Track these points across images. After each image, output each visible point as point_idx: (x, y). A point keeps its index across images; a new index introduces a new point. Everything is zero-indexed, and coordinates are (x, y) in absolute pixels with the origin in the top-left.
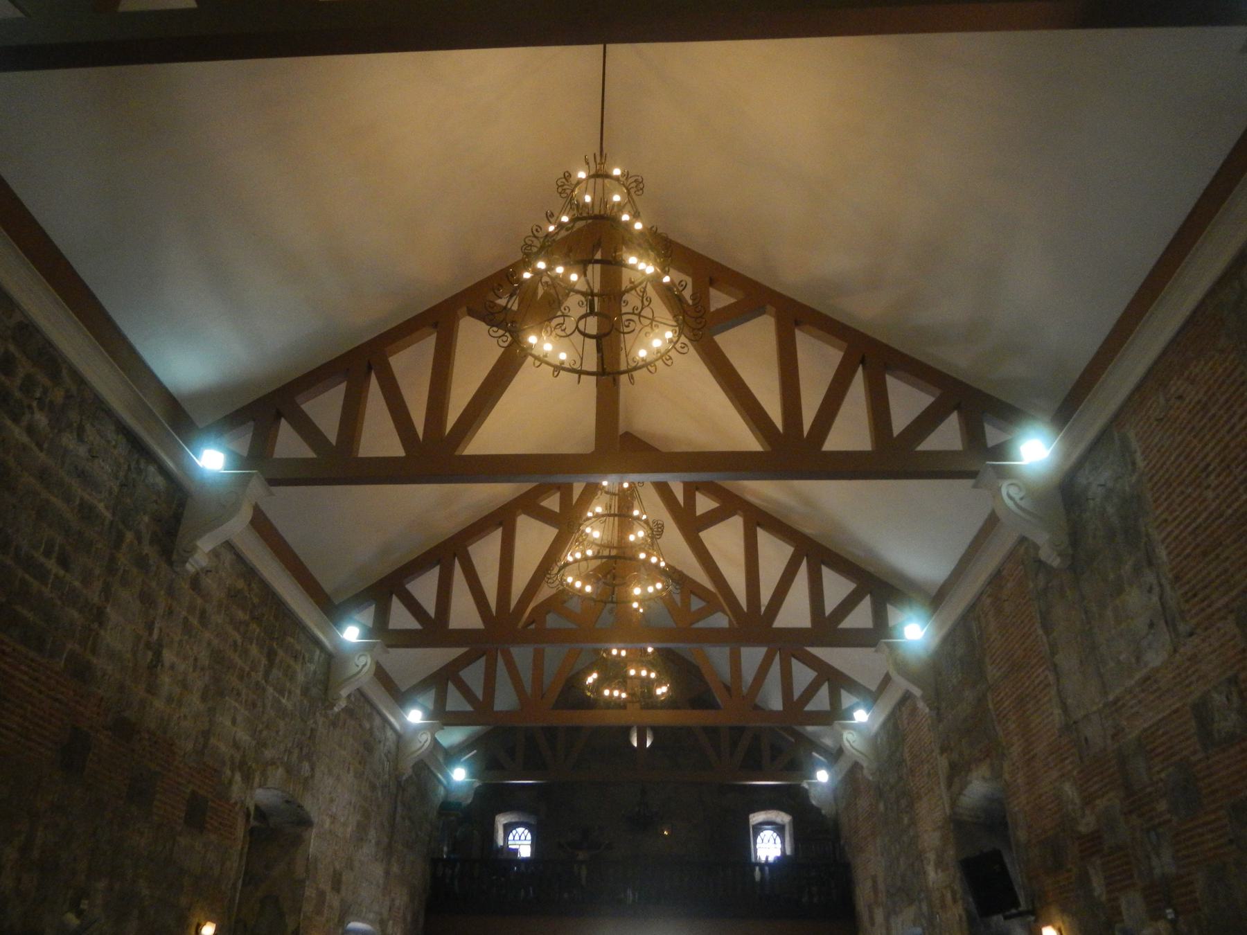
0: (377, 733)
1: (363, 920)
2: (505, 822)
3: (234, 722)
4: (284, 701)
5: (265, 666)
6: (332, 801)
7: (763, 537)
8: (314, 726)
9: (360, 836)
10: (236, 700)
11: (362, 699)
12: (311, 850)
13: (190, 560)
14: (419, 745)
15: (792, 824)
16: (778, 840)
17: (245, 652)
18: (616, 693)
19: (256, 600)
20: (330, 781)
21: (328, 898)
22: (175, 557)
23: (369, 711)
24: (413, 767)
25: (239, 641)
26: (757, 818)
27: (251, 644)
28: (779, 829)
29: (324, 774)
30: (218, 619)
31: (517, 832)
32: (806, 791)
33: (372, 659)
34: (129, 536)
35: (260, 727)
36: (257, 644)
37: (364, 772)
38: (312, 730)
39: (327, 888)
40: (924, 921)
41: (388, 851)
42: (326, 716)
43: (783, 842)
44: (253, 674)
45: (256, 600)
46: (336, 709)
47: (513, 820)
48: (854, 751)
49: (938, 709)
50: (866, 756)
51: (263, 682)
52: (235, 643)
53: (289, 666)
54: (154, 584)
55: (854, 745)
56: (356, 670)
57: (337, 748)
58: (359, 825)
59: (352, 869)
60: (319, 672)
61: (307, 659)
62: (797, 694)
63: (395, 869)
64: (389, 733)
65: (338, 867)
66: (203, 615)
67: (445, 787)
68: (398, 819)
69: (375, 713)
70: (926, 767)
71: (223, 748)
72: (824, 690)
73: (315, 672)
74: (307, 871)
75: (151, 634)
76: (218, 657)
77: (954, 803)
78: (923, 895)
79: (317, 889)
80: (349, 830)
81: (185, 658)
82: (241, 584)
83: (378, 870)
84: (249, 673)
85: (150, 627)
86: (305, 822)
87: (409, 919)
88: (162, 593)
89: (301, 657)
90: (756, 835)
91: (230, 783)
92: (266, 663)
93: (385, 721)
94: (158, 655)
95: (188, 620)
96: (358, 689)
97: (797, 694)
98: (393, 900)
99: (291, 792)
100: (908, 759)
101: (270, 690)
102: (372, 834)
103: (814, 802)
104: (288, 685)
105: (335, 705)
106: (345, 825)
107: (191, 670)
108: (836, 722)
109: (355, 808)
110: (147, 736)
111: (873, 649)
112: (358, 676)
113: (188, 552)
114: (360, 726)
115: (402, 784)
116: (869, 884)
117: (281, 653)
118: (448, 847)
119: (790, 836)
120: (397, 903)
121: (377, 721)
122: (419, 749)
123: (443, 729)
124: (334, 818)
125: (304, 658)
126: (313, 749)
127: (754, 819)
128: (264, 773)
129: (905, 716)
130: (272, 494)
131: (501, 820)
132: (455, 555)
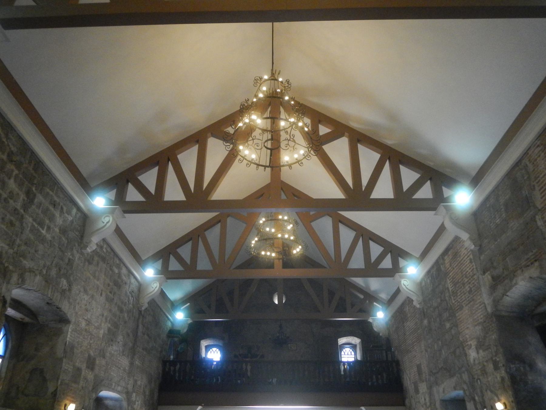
0: (124, 278)
1: (113, 390)
2: (206, 345)
4: (44, 232)
5: (24, 200)
6: (87, 310)
7: (362, 150)
8: (71, 257)
9: (111, 337)
11: (112, 253)
12: (68, 339)
15: (361, 343)
16: (353, 353)
18: (268, 254)
19: (14, 149)
20: (86, 297)
21: (83, 373)
23: (118, 262)
24: (148, 303)
26: (342, 341)
27: (9, 178)
28: (354, 347)
29: (80, 292)
31: (212, 350)
33: (114, 219)
35: (18, 241)
37: (113, 299)
38: (69, 260)
39: (84, 366)
40: (465, 387)
41: (132, 352)
42: (82, 254)
43: (355, 354)
44: (11, 201)
46: (89, 250)
47: (210, 344)
49: (480, 246)
50: (416, 294)
51: (22, 211)
53: (48, 209)
56: (102, 225)
57: (92, 277)
58: (109, 330)
59: (104, 357)
60: (75, 223)
61: (65, 211)
62: (373, 259)
63: (137, 363)
64: (133, 280)
67: (171, 322)
68: (140, 334)
69: (122, 265)
70: (467, 287)
72: (389, 257)
73: (72, 222)
74: (65, 352)
77: (496, 303)
78: (464, 369)
79: (74, 366)
80: (102, 332)
83: (125, 362)
86: (64, 320)
87: (147, 393)
89: (60, 207)
90: (341, 350)
93: (130, 273)
97: (373, 259)
98: (136, 381)
99: (49, 296)
100: (450, 287)
101: (29, 220)
102: (120, 338)
103: (375, 329)
104: (47, 222)
105: (87, 246)
106: (98, 328)
108: (397, 274)
109: (106, 319)
111: (434, 212)
112: (104, 229)
114: (111, 269)
115: (143, 313)
116: (415, 369)
117: (39, 198)
118: (173, 355)
119: (360, 350)
120: (139, 383)
121: (124, 271)
122: (152, 292)
123: (167, 282)
124: (89, 322)
125: (62, 208)
126: (70, 272)
127: (340, 341)
128: (22, 276)
129: (446, 262)
131: (204, 343)
132: (169, 160)
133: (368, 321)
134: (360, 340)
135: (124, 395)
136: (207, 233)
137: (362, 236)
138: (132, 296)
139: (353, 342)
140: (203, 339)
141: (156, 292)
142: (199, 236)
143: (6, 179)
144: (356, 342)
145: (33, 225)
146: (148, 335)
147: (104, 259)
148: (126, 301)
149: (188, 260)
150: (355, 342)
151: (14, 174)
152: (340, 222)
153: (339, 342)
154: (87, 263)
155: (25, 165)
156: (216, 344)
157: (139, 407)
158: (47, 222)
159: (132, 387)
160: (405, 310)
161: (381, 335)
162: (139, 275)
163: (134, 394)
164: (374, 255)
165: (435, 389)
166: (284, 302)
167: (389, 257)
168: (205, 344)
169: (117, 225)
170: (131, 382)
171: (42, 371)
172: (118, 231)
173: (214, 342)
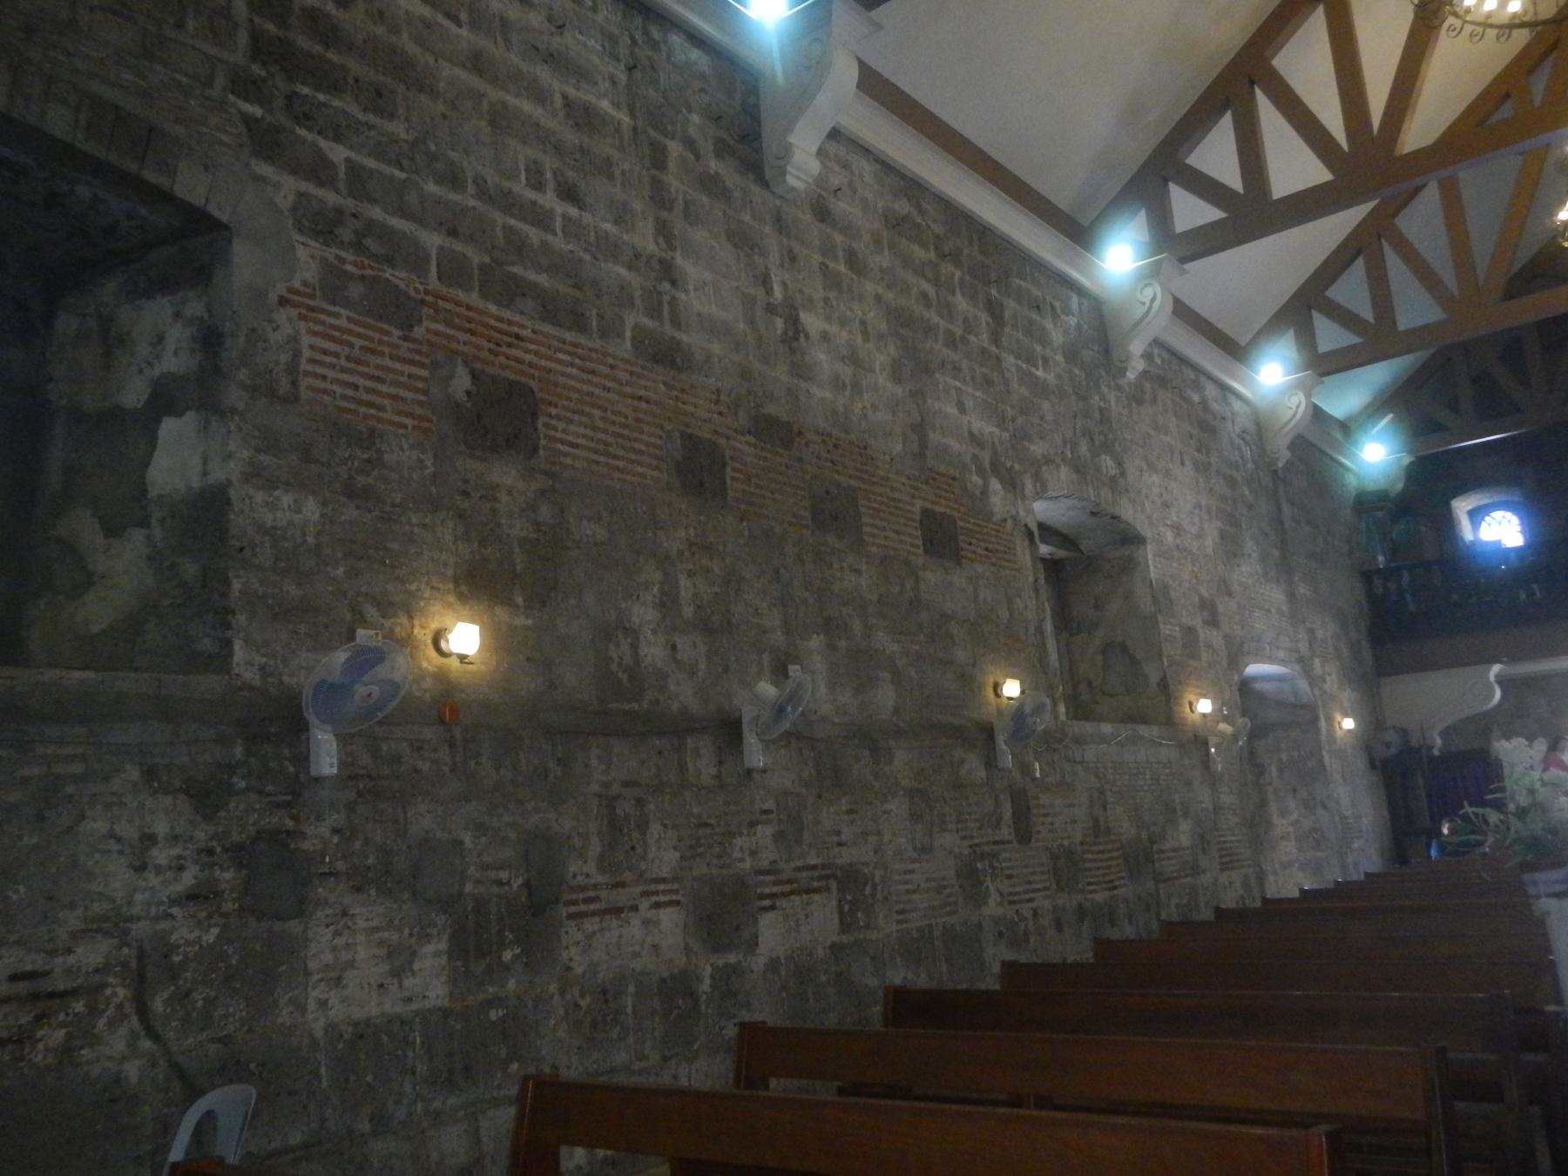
0: (1215, 407)
1: (1270, 660)
2: (1469, 508)
3: (962, 408)
4: (1040, 373)
5: (988, 324)
6: (1166, 505)
8: (1102, 404)
9: (1230, 546)
10: (955, 378)
11: (1175, 361)
12: (1152, 575)
13: (789, 168)
17: (947, 310)
20: (1155, 478)
22: (768, 174)
23: (1192, 376)
24: (1288, 448)
25: (931, 292)
27: (954, 294)
29: (1141, 471)
30: (884, 260)
33: (1164, 288)
34: (674, 148)
35: (1010, 412)
36: (963, 294)
38: (1101, 411)
39: (1197, 622)
41: (1283, 568)
42: (1119, 388)
44: (972, 338)
45: (938, 229)
46: (1131, 375)
47: (1482, 502)
51: (993, 348)
52: (924, 295)
53: (1031, 322)
54: (747, 218)
57: (1152, 432)
58: (1223, 535)
59: (1230, 595)
60: (1086, 327)
61: (1059, 311)
63: (1303, 590)
64: (1237, 405)
65: (1205, 594)
66: (852, 258)
68: (1288, 523)
69: (1203, 379)
71: (954, 445)
73: (1079, 326)
74: (1155, 601)
75: (769, 291)
76: (899, 319)
79: (1180, 625)
80: (1209, 542)
81: (844, 322)
82: (902, 207)
83: (1276, 595)
84: (963, 338)
85: (765, 281)
86: (1130, 539)
87: (1346, 652)
88: (767, 229)
89: (1049, 308)
91: (985, 492)
92: (990, 320)
93: (1224, 388)
94: (794, 322)
95: (827, 267)
96: (1154, 340)
98: (1311, 632)
99: (1093, 499)
101: (1010, 360)
102: (1250, 545)
104: (1039, 348)
105: (1126, 369)
106: (1199, 536)
107: (859, 340)
109: (1209, 512)
110: (818, 439)
112: (1148, 319)
113: (782, 158)
114: (1184, 399)
115: (1280, 473)
117: (1010, 305)
118: (1385, 555)
120: (1320, 634)
121: (1211, 391)
122: (1294, 416)
123: (1323, 382)
124: (1178, 530)
125: (1053, 308)
126: (1111, 436)
128: (1037, 476)
130: (878, 26)
131: (1462, 507)
132: (1252, 82)
135: (1297, 667)
138: (1247, 444)
141: (1300, 420)
143: (950, 298)
145: (1019, 369)
146: (1308, 522)
147: (1162, 382)
148: (1238, 458)
149: (1367, 314)
151: (957, 278)
154: (1134, 405)
155: (966, 252)
157: (1336, 686)
158: (1039, 348)
159: (1308, 646)
163: (1317, 662)
169: (1173, 295)
170: (1303, 635)
171: (1124, 648)
172: (1182, 311)
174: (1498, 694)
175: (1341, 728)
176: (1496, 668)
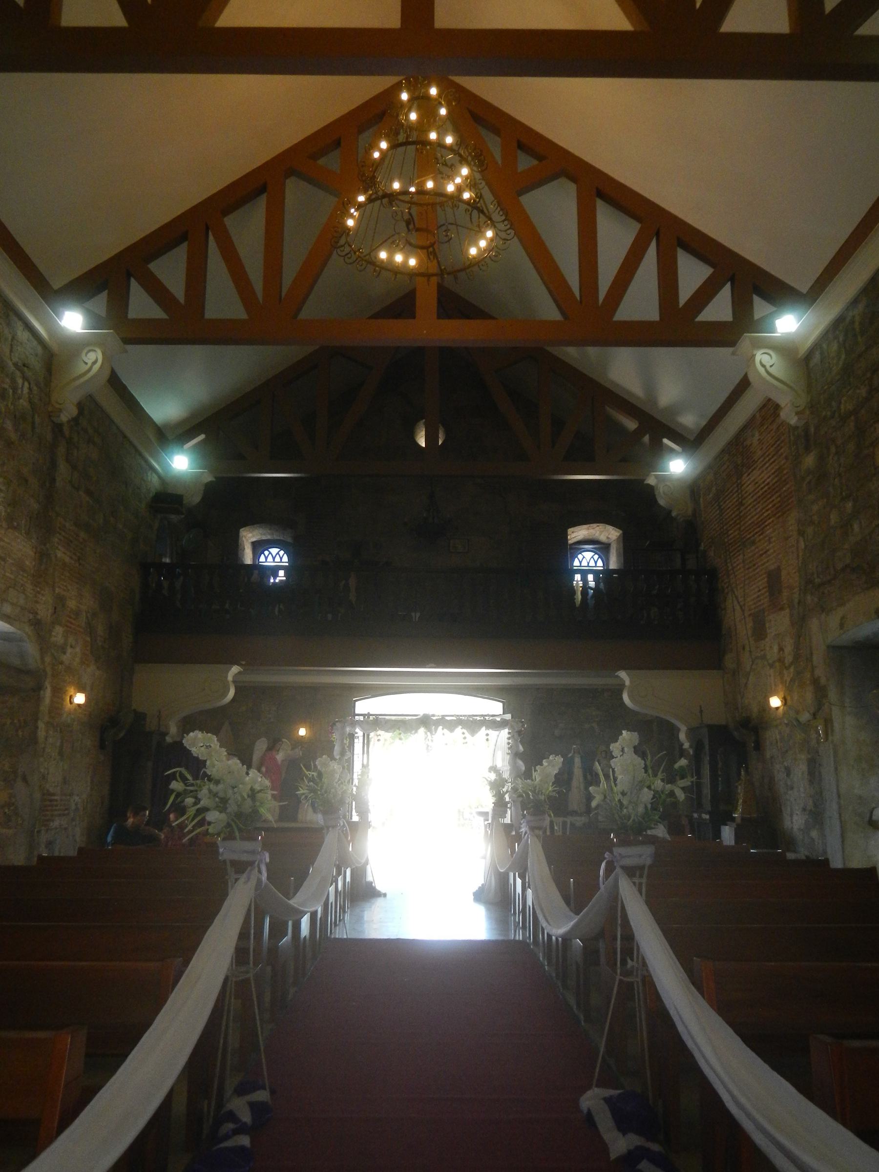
2: (254, 539)
14: (83, 368)
15: (622, 538)
18: (399, 258)
26: (577, 534)
28: (602, 548)
31: (270, 553)
32: (651, 488)
47: (264, 538)
48: (768, 378)
50: (791, 387)
55: (772, 370)
67: (159, 477)
72: (725, 293)
98: (60, 600)
108: (745, 334)
115: (66, 430)
119: (618, 555)
120: (72, 604)
127: (573, 535)
131: (249, 536)
133: (646, 482)
134: (621, 532)
135: (28, 629)
136: (229, 221)
137: (658, 234)
138: (25, 378)
139: (603, 538)
140: (245, 525)
142: (207, 229)
144: (610, 536)
146: (89, 493)
148: (6, 386)
150: (608, 538)
152: (601, 194)
153: (569, 537)
156: (279, 538)
157: (77, 660)
159: (51, 611)
160: (748, 443)
161: (674, 514)
162: (42, 324)
163: (59, 630)
164: (687, 288)
165: (814, 624)
166: (440, 444)
167: (725, 293)
168: (251, 537)
173: (273, 534)
174: (232, 693)
175: (71, 703)
176: (235, 669)
